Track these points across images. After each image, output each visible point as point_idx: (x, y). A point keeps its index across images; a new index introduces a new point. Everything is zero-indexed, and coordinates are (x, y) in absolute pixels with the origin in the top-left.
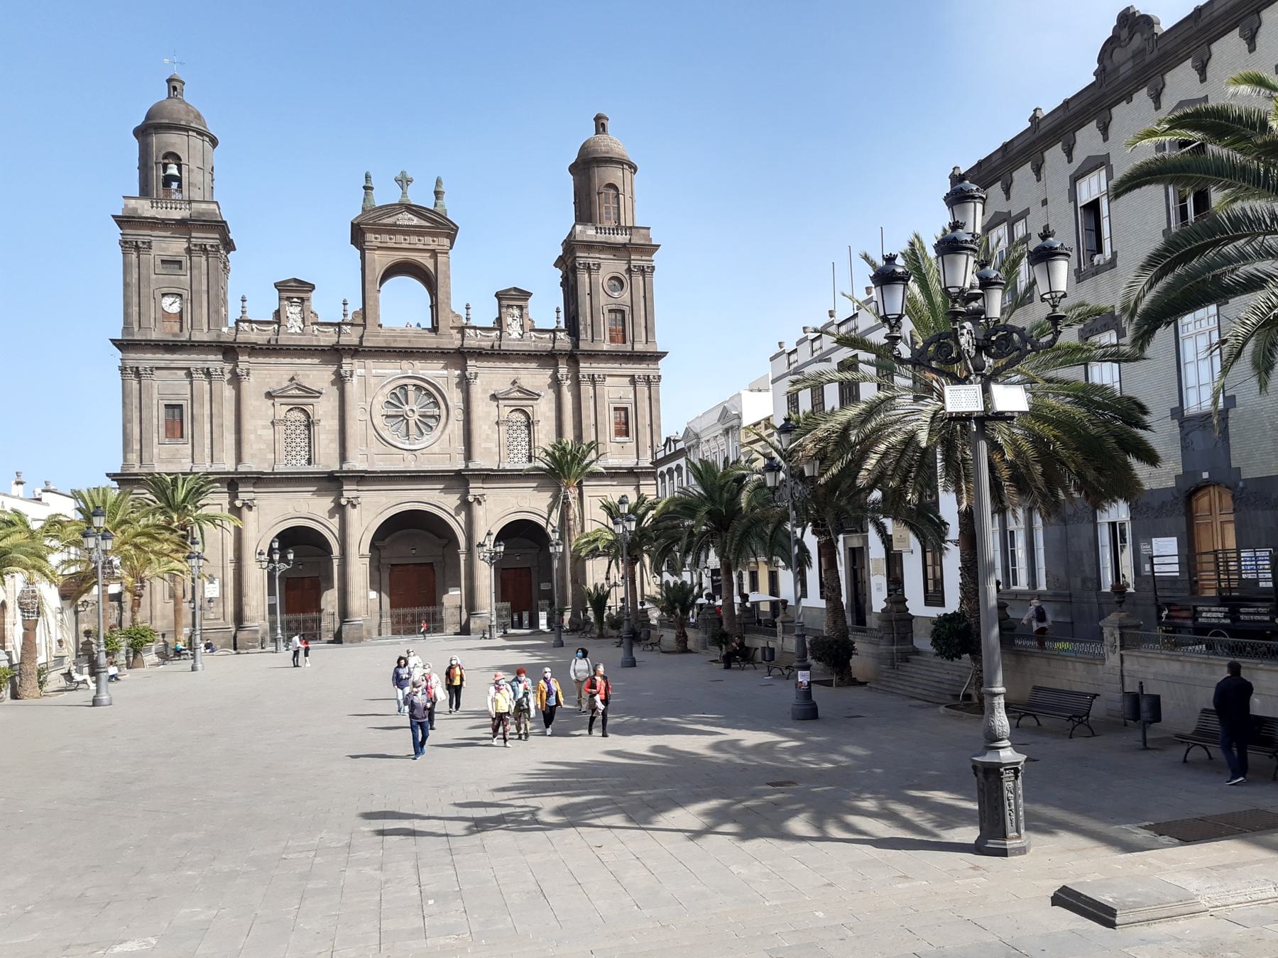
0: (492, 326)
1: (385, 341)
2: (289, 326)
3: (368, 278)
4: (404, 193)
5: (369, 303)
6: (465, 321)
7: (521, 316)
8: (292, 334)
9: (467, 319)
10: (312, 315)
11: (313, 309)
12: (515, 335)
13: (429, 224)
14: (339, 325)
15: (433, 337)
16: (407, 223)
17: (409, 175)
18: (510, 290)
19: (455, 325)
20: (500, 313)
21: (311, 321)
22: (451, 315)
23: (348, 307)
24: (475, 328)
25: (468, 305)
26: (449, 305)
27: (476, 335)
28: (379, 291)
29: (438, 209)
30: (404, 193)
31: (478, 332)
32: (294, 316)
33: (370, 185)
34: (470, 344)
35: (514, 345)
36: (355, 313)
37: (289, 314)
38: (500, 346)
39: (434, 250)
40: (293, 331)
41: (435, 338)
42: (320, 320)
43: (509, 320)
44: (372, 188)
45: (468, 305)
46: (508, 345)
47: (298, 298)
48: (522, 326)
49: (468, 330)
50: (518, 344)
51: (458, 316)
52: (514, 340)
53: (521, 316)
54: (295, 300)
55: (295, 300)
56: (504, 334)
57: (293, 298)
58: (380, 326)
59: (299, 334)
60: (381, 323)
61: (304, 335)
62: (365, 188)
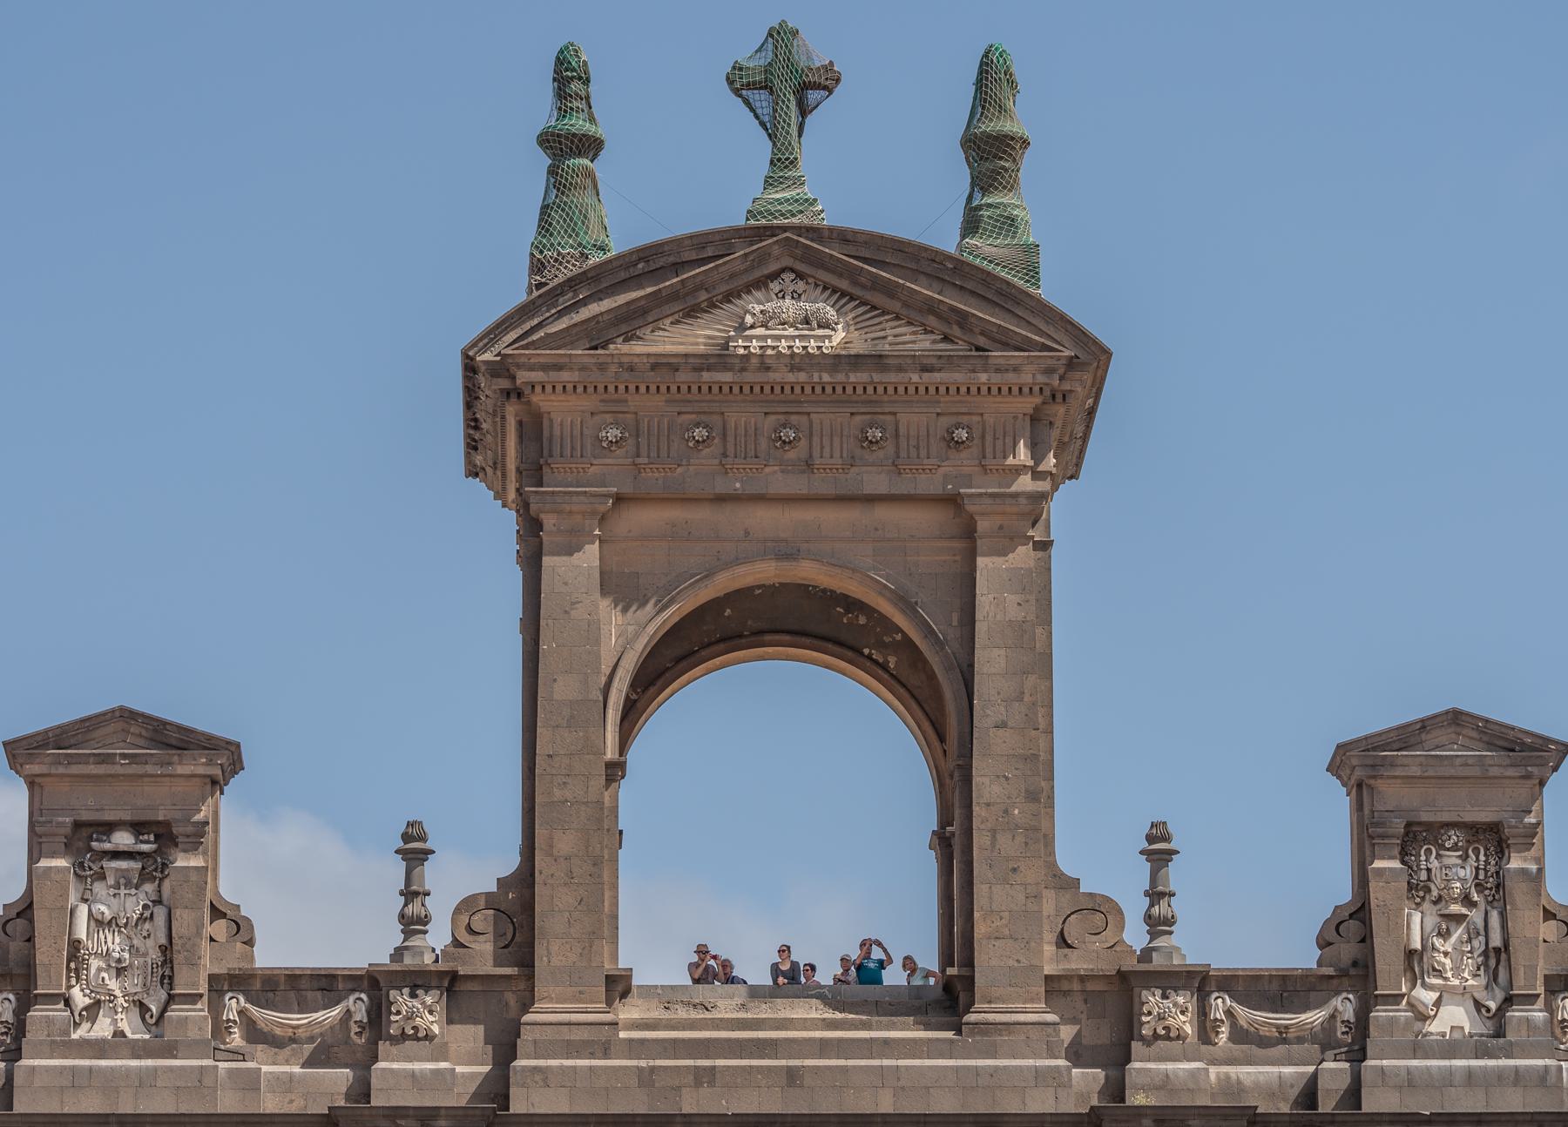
0: (1303, 956)
1: (646, 1078)
2: (80, 999)
3: (560, 688)
4: (782, 164)
5: (561, 841)
6: (1135, 936)
7: (1496, 889)
8: (98, 1048)
9: (1158, 925)
10: (220, 929)
11: (228, 889)
12: (1454, 1018)
13: (923, 344)
14: (374, 983)
15: (930, 1049)
16: (788, 341)
17: (816, 49)
18: (1424, 725)
19: (1077, 963)
20: (1362, 879)
21: (209, 964)
22: (1050, 904)
23: (431, 874)
24: (1201, 982)
25: (1158, 833)
26: (1041, 838)
27: (1206, 1031)
28: (615, 771)
29: (986, 249)
30: (782, 164)
31: (1220, 1004)
32: (114, 943)
33: (578, 124)
34: (1165, 1084)
35: (1448, 1077)
36: (467, 905)
37: (81, 932)
38: (1354, 1094)
39: (953, 501)
40: (102, 1028)
41: (948, 1050)
42: (269, 955)
43: (1417, 924)
44: (590, 146)
45: (1158, 833)
46: (1411, 1082)
47: (138, 828)
48: (1496, 959)
49: (1152, 1000)
50: (1470, 1076)
51: (1103, 910)
52: (1449, 1048)
53: (1496, 889)
54: (123, 839)
55: (123, 839)
56: (1380, 1013)
57: (108, 828)
58: (618, 986)
59: (139, 1050)
60: (622, 964)
61: (170, 1051)
62: (549, 141)
